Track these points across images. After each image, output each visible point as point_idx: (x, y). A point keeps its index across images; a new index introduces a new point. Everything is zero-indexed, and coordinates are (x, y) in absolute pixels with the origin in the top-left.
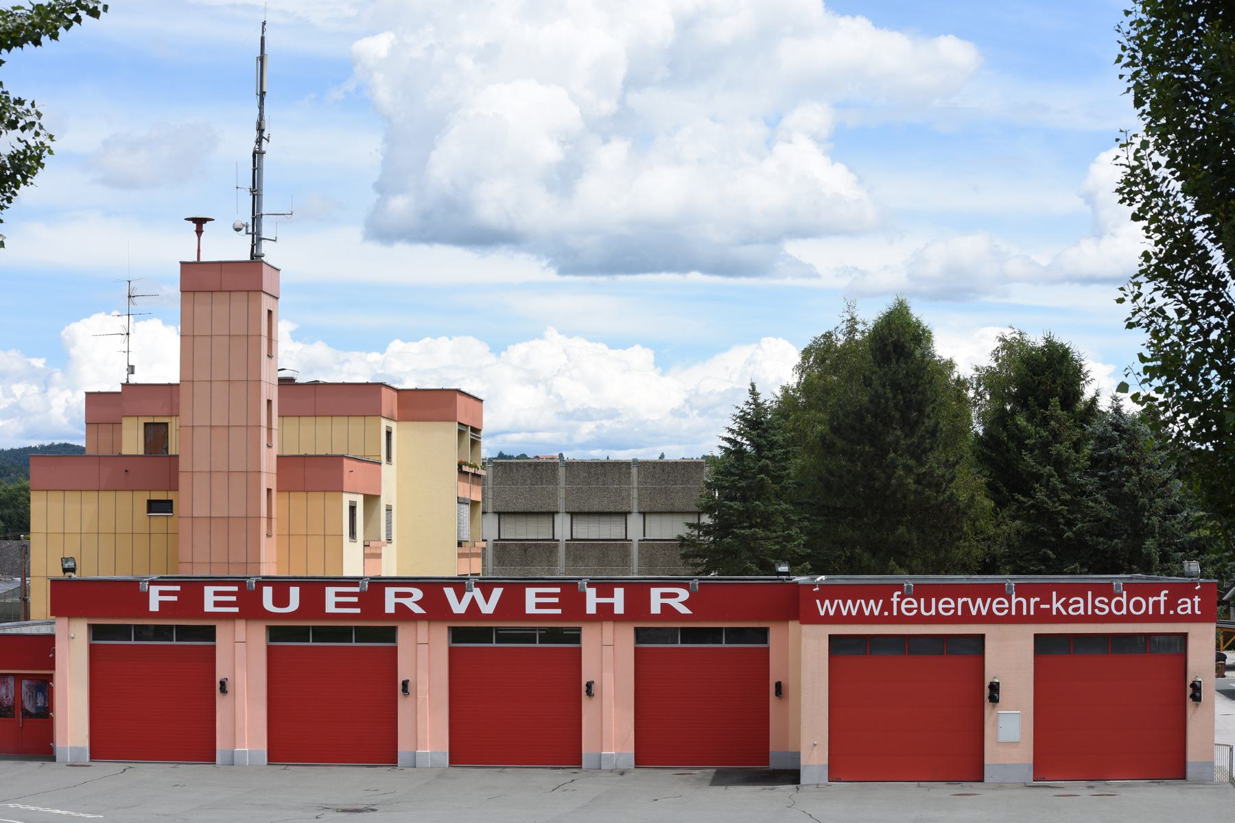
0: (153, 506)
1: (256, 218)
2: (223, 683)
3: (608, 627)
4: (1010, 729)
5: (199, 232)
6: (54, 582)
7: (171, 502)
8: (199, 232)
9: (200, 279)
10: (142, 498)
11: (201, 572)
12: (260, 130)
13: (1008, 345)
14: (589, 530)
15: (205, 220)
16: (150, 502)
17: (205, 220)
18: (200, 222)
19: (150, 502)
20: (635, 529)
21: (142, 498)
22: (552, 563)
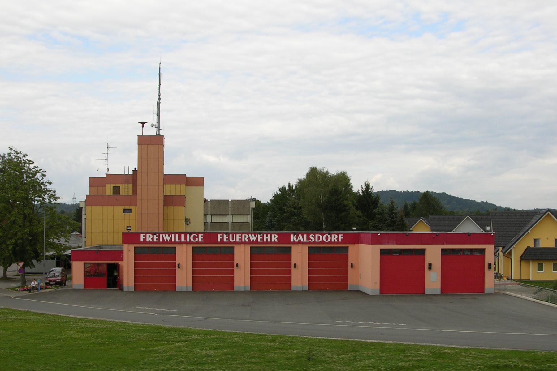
0: (125, 210)
1: (158, 122)
2: (179, 265)
3: (242, 246)
4: (433, 280)
5: (143, 126)
6: (124, 234)
7: (131, 209)
8: (143, 126)
9: (143, 140)
10: (122, 208)
11: (181, 232)
12: (159, 95)
13: (313, 172)
14: (216, 219)
15: (145, 123)
16: (124, 209)
17: (145, 123)
18: (143, 123)
19: (124, 209)
20: (230, 219)
21: (122, 208)
22: (227, 229)
